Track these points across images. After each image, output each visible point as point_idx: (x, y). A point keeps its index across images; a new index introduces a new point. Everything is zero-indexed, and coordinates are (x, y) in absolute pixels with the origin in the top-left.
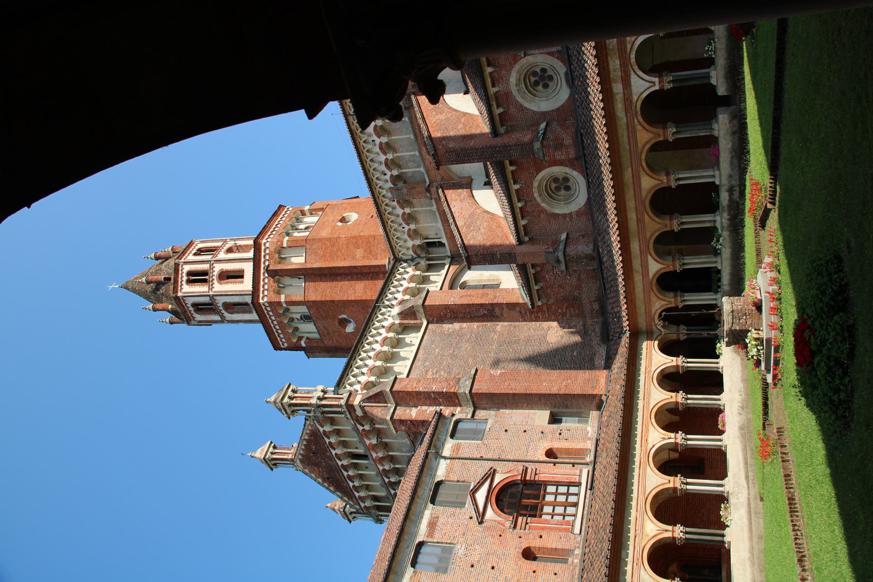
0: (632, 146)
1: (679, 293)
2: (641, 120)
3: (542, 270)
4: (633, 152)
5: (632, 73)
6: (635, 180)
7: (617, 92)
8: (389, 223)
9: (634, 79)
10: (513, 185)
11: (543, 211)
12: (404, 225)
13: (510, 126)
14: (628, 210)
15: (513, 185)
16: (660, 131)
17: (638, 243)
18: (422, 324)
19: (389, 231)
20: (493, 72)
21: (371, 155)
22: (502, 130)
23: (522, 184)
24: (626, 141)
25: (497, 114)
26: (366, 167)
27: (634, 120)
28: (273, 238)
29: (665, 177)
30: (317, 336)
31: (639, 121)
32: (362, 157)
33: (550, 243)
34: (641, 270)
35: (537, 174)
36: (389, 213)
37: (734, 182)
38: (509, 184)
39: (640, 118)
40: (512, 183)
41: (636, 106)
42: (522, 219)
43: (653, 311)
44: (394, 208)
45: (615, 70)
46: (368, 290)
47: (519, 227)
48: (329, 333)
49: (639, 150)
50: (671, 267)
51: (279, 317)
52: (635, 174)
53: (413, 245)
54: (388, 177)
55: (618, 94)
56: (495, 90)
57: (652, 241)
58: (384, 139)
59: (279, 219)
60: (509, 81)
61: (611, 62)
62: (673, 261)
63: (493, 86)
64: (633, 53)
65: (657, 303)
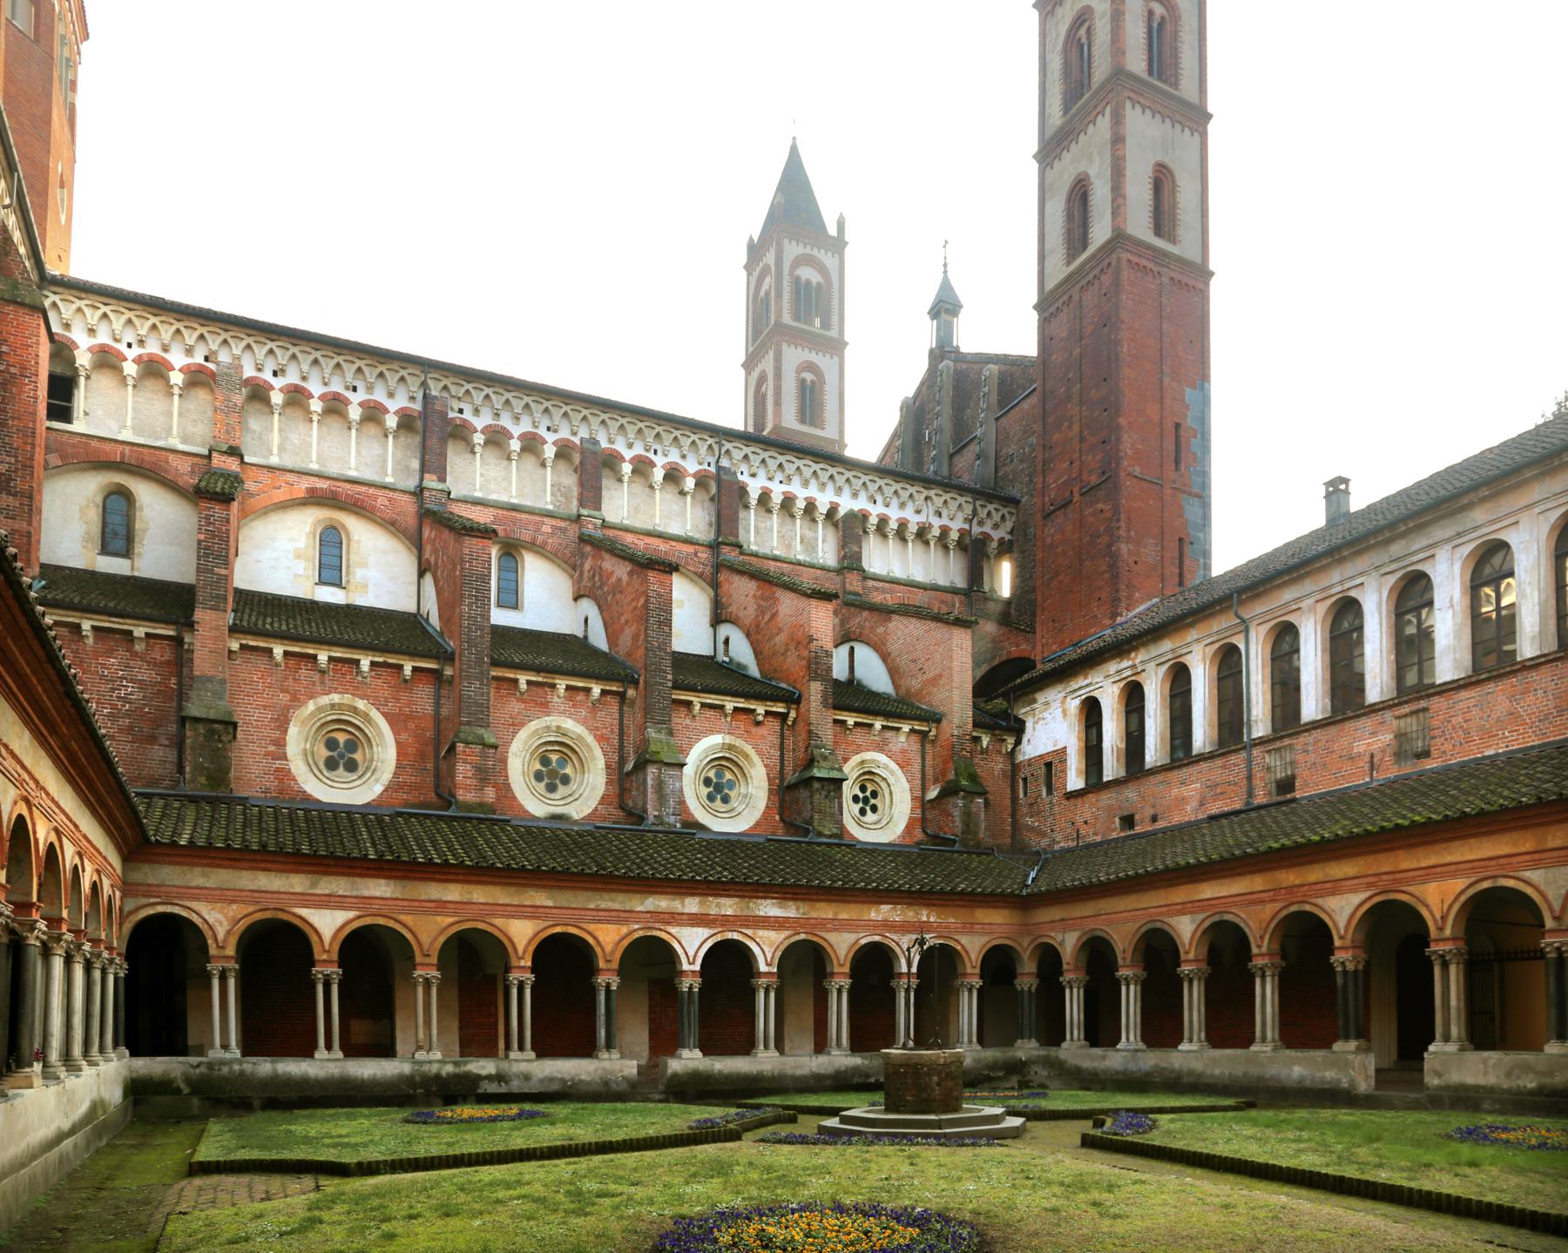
0: (595, 913)
2: (636, 935)
3: (134, 654)
10: (370, 658)
11: (297, 700)
14: (466, 886)
16: (615, 965)
24: (603, 906)
27: (637, 922)
39: (641, 933)
40: (377, 659)
43: (194, 905)
45: (718, 905)
49: (584, 926)
50: (325, 957)
52: (541, 910)
55: (683, 906)
57: (391, 924)
63: (568, 688)
65: (220, 917)
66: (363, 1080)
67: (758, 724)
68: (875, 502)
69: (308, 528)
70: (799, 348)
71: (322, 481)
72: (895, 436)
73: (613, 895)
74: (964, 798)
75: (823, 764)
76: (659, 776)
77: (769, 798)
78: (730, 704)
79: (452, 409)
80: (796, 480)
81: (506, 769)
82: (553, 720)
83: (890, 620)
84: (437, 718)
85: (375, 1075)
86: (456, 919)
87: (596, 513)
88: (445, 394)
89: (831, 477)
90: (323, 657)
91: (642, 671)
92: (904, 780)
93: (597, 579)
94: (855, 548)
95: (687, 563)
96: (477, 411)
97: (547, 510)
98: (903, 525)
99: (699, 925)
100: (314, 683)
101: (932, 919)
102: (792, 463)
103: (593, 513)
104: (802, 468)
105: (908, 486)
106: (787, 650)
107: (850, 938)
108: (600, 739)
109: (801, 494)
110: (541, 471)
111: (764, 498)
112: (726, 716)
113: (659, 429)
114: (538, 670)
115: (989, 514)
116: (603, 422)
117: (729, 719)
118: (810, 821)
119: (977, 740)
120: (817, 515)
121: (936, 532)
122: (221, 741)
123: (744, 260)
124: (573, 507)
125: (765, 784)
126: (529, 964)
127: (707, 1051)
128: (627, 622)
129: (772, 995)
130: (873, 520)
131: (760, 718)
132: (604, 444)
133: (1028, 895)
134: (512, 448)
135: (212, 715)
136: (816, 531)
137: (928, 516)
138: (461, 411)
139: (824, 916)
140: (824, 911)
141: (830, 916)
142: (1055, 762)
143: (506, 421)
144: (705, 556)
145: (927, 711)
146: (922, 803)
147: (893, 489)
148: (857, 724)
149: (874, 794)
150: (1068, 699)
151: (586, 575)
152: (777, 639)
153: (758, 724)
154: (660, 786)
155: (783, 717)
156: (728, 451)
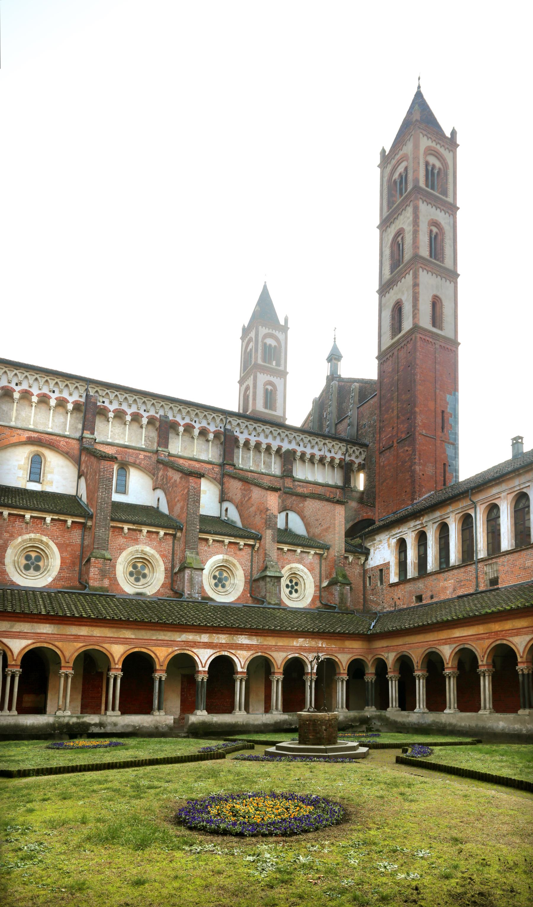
0: (156, 642)
2: (176, 653)
4: (149, 641)
5: (214, 651)
6: (122, 640)
9: (210, 652)
16: (165, 668)
24: (160, 638)
25: (124, 526)
31: (176, 650)
35: (56, 544)
39: (178, 652)
40: (54, 517)
41: (189, 650)
45: (218, 638)
52: (128, 640)
55: (201, 638)
66: (27, 727)
67: (241, 549)
68: (299, 445)
69: (26, 455)
70: (265, 375)
71: (35, 433)
72: (310, 415)
73: (166, 633)
74: (340, 586)
75: (271, 569)
76: (191, 575)
77: (245, 586)
78: (227, 540)
79: (99, 401)
80: (262, 435)
81: (115, 571)
82: (139, 547)
83: (306, 501)
84: (82, 546)
85: (33, 723)
87: (166, 450)
88: (96, 395)
89: (279, 434)
90: (28, 516)
91: (185, 524)
92: (311, 577)
93: (165, 480)
94: (290, 467)
95: (208, 473)
96: (111, 402)
97: (142, 448)
98: (313, 456)
99: (208, 648)
100: (22, 529)
101: (324, 646)
102: (260, 427)
103: (164, 449)
104: (265, 429)
105: (315, 438)
106: (256, 515)
108: (163, 556)
109: (264, 441)
110: (140, 430)
111: (247, 443)
112: (225, 546)
113: (197, 411)
114: (134, 523)
115: (354, 451)
116: (171, 408)
117: (226, 547)
118: (264, 597)
119: (346, 558)
120: (272, 451)
121: (328, 459)
123: (241, 335)
124: (155, 447)
125: (243, 579)
126: (121, 667)
127: (210, 711)
128: (178, 501)
129: (244, 683)
130: (299, 454)
131: (242, 547)
132: (171, 418)
133: (371, 634)
134: (127, 419)
136: (271, 459)
137: (324, 452)
138: (103, 402)
139: (270, 644)
140: (271, 641)
141: (274, 644)
142: (384, 569)
143: (125, 407)
144: (217, 470)
145: (323, 544)
146: (320, 589)
147: (308, 439)
148: (288, 550)
149: (296, 584)
150: (391, 539)
151: (159, 478)
152: (251, 509)
153: (240, 549)
154: (191, 579)
155: (253, 546)
156: (230, 422)
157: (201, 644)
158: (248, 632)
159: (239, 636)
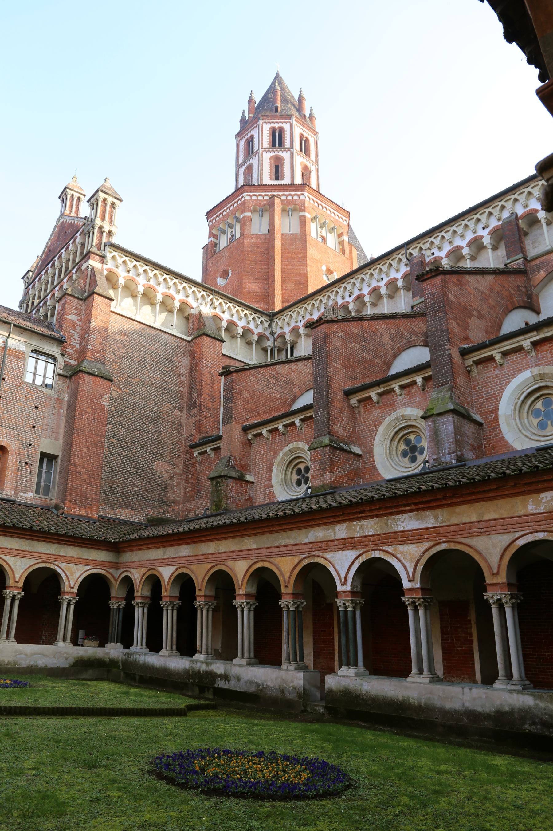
0: (278, 549)
1: (148, 601)
4: (271, 550)
5: (358, 553)
7: (337, 531)
8: (305, 306)
9: (351, 554)
10: (299, 418)
12: (303, 322)
13: (359, 412)
15: (299, 418)
16: (290, 590)
17: (187, 554)
18: (190, 336)
19: (297, 306)
20: (418, 386)
21: (368, 278)
22: (353, 401)
23: (301, 429)
24: (283, 543)
25: (370, 394)
26: (355, 274)
28: (310, 203)
29: (244, 592)
30: (217, 251)
32: (365, 269)
33: (243, 463)
34: (166, 557)
36: (313, 304)
37: (233, 682)
38: (300, 414)
42: (267, 431)
44: (318, 309)
45: (361, 527)
46: (252, 294)
47: (260, 428)
48: (217, 262)
49: (272, 560)
51: (232, 214)
52: (250, 552)
53: (285, 333)
54: (347, 299)
55: (335, 533)
56: (398, 391)
58: (383, 291)
59: (332, 210)
60: (407, 407)
61: (372, 523)
62: (170, 596)
63: (402, 387)
64: (382, 556)
73: (289, 533)
81: (373, 456)
86: (213, 564)
107: (503, 540)
122: (220, 486)
135: (216, 474)
139: (466, 520)
157: (336, 543)
158: (408, 505)
159: (397, 517)
